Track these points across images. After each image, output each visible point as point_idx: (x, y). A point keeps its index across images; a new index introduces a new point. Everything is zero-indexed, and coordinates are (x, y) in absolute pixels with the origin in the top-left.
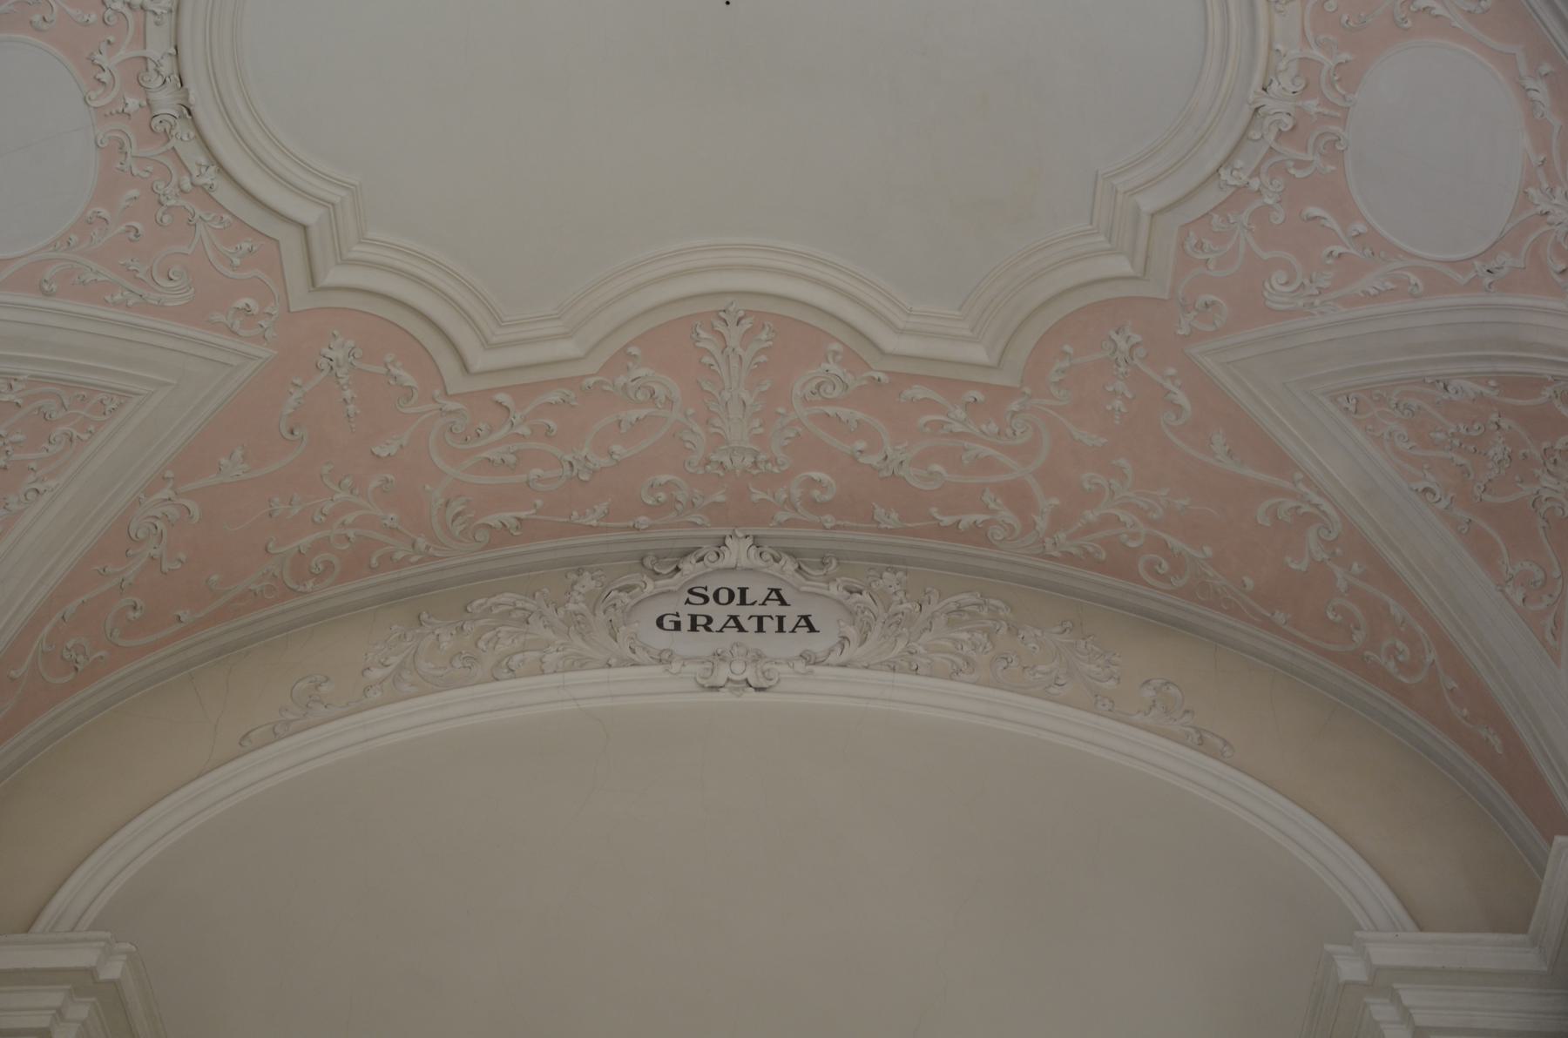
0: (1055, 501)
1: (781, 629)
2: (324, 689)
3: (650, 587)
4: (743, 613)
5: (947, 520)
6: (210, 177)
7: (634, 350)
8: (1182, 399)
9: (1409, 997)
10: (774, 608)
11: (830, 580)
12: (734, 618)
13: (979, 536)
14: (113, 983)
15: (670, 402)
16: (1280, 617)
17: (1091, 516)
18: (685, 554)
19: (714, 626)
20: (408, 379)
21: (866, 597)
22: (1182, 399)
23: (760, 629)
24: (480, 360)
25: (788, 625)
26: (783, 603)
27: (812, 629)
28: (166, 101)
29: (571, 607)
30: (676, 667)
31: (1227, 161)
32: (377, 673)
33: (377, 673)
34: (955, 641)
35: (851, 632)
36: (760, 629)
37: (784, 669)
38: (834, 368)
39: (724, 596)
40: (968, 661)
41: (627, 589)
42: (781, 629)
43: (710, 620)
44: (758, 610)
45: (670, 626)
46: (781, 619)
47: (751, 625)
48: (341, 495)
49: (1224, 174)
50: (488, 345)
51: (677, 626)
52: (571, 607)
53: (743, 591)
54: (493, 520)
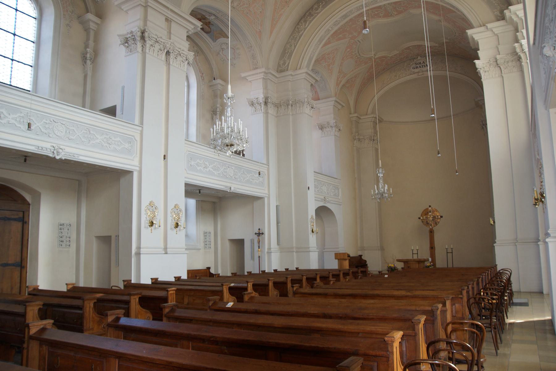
1: (424, 67)
3: (412, 63)
4: (421, 65)
6: (364, 58)
10: (423, 64)
12: (420, 66)
18: (414, 58)
19: (418, 67)
23: (423, 67)
25: (425, 66)
26: (424, 63)
29: (404, 68)
32: (388, 79)
36: (423, 67)
44: (422, 65)
46: (424, 65)
47: (421, 67)
51: (415, 68)
52: (404, 68)
53: (420, 63)
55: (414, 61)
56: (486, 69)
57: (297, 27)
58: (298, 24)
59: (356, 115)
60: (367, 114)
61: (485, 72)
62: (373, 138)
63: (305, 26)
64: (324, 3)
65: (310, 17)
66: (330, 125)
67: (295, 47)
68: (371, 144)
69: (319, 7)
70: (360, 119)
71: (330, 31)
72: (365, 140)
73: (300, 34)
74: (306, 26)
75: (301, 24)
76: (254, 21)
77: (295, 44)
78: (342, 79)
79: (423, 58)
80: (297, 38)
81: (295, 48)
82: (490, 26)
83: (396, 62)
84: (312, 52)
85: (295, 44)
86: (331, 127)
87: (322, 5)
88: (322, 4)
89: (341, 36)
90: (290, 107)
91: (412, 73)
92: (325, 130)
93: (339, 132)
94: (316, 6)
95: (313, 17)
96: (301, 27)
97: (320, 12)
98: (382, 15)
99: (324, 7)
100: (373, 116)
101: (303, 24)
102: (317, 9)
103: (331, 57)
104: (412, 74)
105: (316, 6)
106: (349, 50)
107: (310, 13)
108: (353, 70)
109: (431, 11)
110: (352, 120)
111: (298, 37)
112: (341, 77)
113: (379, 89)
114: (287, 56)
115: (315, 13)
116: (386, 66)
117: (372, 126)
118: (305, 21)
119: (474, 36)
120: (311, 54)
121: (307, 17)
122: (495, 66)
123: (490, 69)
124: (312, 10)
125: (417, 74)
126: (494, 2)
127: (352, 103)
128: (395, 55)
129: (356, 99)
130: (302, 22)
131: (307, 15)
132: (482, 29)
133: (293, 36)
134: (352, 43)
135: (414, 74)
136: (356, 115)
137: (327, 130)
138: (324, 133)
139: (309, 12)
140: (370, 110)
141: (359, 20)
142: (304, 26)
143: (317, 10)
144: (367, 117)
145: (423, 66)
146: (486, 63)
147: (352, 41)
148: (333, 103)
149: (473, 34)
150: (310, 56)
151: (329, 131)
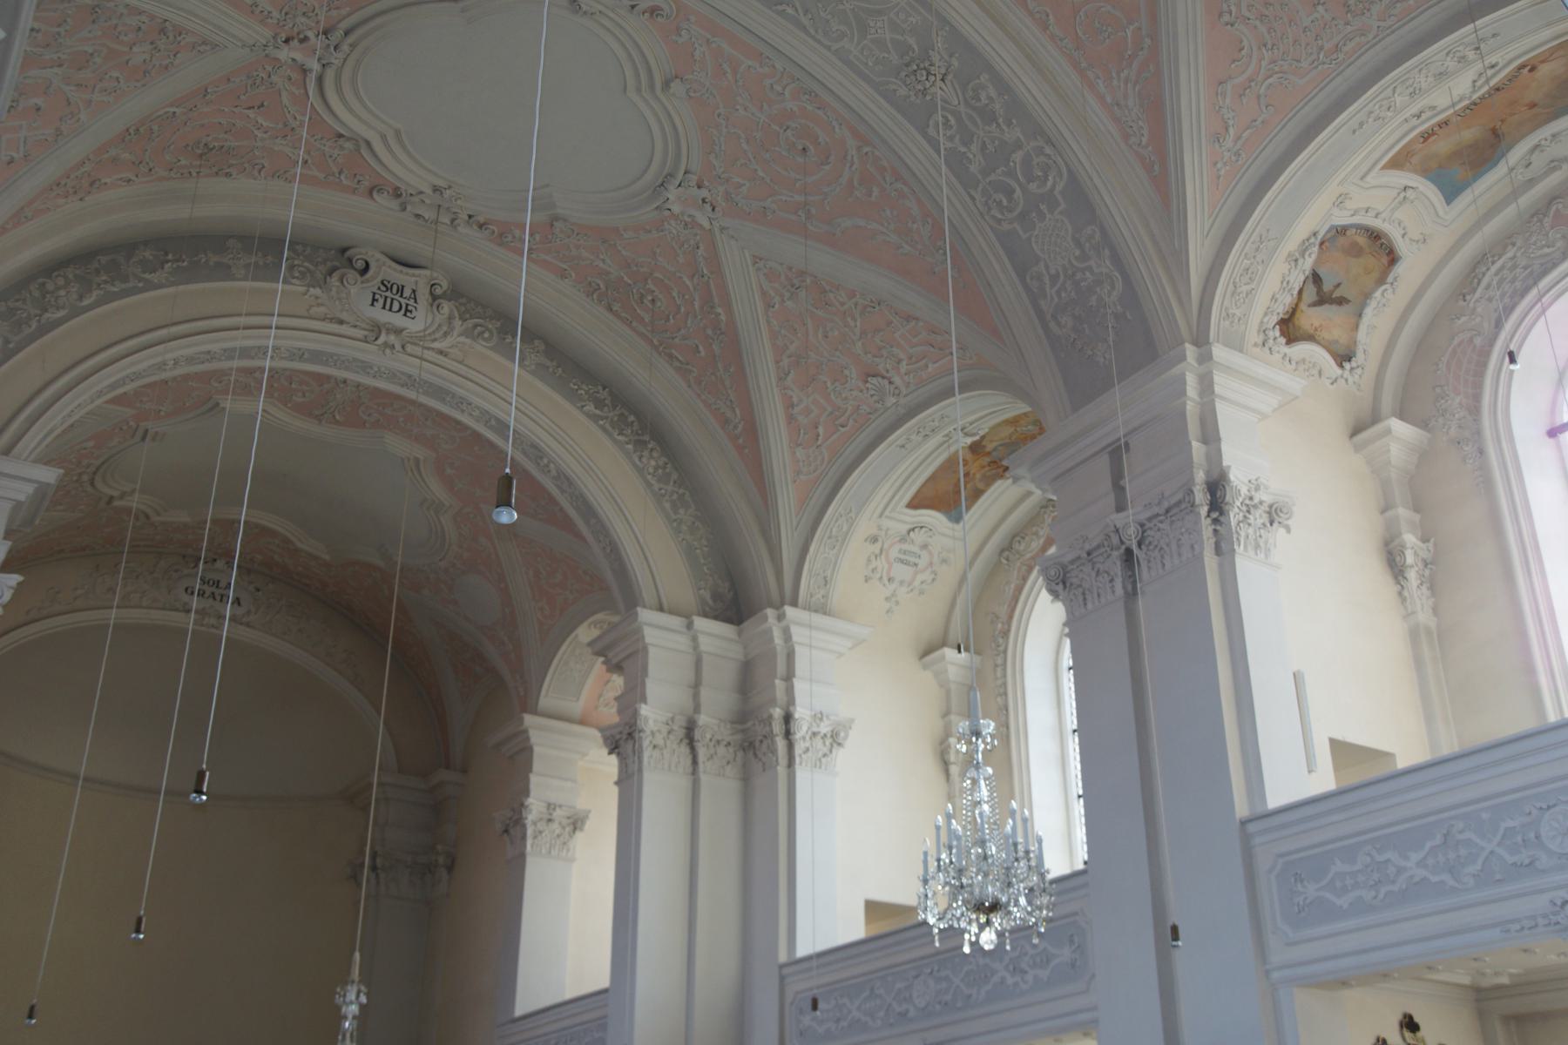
4: (217, 592)
12: (213, 593)
19: (206, 595)
21: (260, 593)
36: (221, 600)
39: (211, 583)
41: (176, 571)
43: (204, 593)
47: (218, 598)
53: (218, 582)
56: (659, 740)
57: (41, 280)
61: (655, 747)
63: (81, 298)
64: (185, 263)
69: (163, 268)
73: (47, 315)
74: (86, 302)
75: (61, 281)
80: (30, 327)
82: (701, 623)
85: (11, 346)
88: (177, 261)
94: (148, 254)
95: (123, 286)
96: (62, 293)
97: (160, 286)
104: (177, 610)
109: (449, 471)
111: (34, 325)
119: (647, 631)
121: (97, 272)
122: (681, 740)
123: (668, 742)
126: (702, 561)
130: (71, 276)
132: (676, 622)
142: (75, 296)
143: (151, 273)
146: (663, 723)
149: (646, 624)
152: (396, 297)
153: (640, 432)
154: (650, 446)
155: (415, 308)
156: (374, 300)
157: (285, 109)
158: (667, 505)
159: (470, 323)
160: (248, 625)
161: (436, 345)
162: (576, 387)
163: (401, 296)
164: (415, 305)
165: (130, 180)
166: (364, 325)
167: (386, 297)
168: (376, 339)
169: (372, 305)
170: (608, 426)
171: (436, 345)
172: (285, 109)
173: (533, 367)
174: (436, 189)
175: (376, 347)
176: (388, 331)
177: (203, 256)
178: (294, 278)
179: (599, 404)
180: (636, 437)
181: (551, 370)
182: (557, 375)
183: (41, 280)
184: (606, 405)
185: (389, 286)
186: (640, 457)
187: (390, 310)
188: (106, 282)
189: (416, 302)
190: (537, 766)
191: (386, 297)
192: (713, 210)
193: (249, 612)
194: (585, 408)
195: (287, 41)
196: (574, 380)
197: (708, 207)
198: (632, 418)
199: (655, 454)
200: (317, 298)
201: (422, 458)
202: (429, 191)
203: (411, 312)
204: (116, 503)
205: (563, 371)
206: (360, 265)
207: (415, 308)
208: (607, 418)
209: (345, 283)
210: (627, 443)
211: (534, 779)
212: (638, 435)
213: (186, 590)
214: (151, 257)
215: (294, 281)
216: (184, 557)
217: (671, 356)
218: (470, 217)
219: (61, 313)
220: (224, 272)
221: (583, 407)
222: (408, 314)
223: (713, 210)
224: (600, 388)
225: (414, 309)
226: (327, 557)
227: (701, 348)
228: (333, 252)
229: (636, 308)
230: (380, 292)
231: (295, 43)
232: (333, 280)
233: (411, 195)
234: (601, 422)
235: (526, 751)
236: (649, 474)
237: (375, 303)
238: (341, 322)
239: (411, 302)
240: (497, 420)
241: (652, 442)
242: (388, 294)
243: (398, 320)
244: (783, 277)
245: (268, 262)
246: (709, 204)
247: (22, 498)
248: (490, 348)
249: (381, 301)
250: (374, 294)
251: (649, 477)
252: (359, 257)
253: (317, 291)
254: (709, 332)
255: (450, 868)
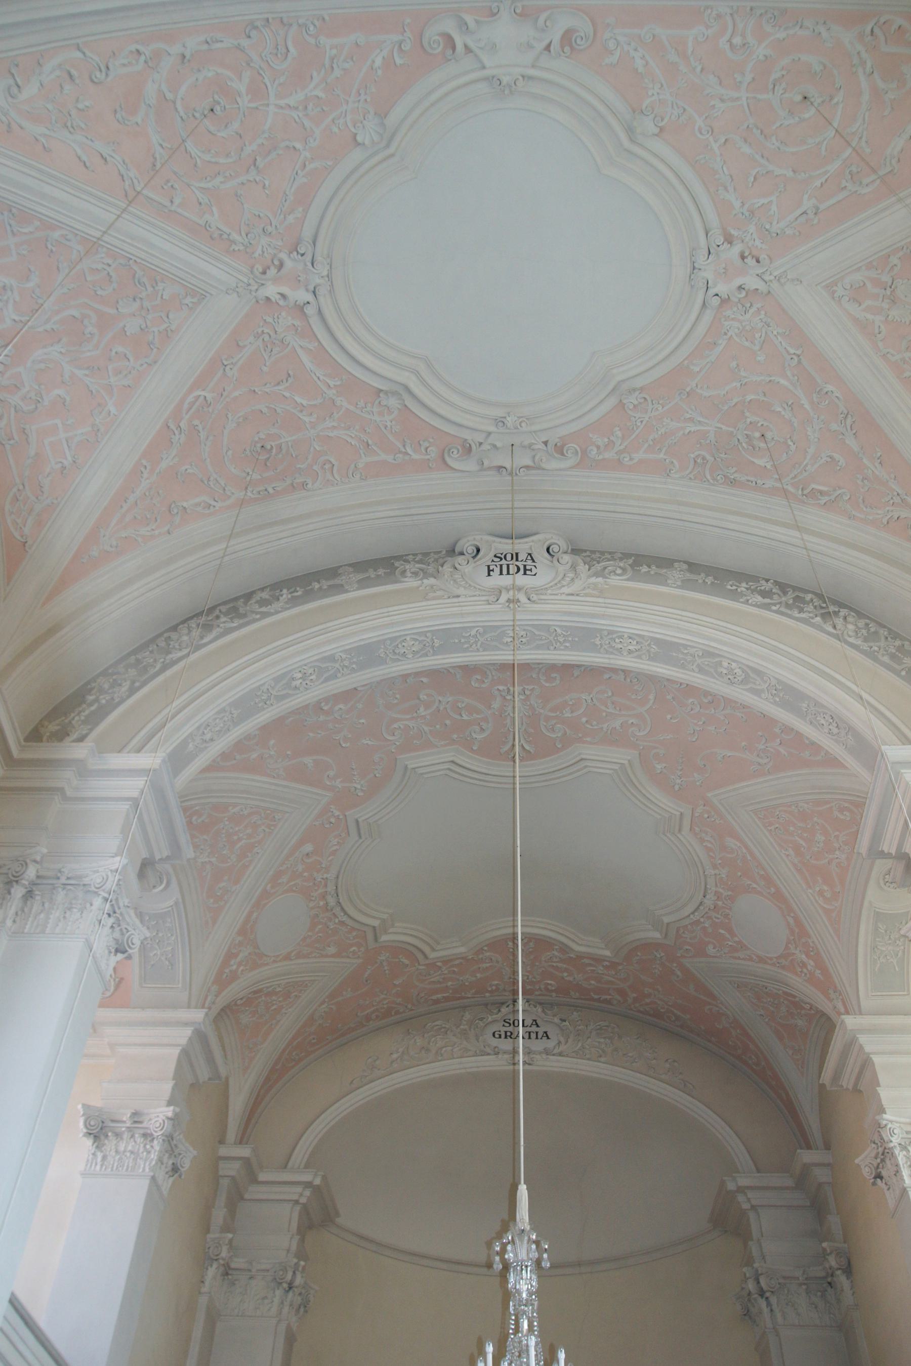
0: (635, 995)
1: (537, 1038)
2: (377, 1062)
3: (490, 1019)
5: (596, 997)
6: (345, 918)
7: (486, 948)
8: (679, 973)
9: (750, 1194)
10: (534, 1028)
11: (554, 1016)
13: (608, 1002)
14: (318, 1186)
15: (498, 962)
16: (713, 1039)
17: (648, 1001)
18: (503, 1004)
20: (406, 962)
21: (567, 1023)
22: (679, 973)
23: (530, 1038)
24: (432, 955)
25: (540, 1036)
26: (538, 1026)
27: (548, 1038)
28: (332, 901)
29: (462, 1027)
30: (500, 1056)
31: (693, 913)
32: (395, 1056)
33: (395, 1056)
34: (599, 1042)
35: (562, 1039)
36: (530, 1038)
37: (538, 1057)
38: (556, 953)
40: (603, 1051)
41: (481, 1019)
42: (537, 1038)
43: (512, 1033)
44: (529, 1029)
45: (497, 1036)
46: (537, 1033)
48: (383, 996)
49: (692, 916)
50: (433, 950)
52: (462, 1027)
54: (434, 997)
55: (499, 1011)
58: (174, 628)
59: (245, 1152)
60: (285, 1167)
62: (289, 1277)
63: (202, 638)
65: (231, 619)
66: (144, 1125)
67: (132, 691)
68: (277, 1300)
70: (254, 1181)
71: (296, 688)
72: (251, 1278)
73: (170, 656)
74: (205, 640)
76: (21, 487)
77: (137, 684)
78: (242, 968)
79: (535, 1007)
81: (129, 697)
83: (439, 996)
84: (198, 728)
85: (137, 684)
86: (145, 1135)
87: (289, 596)
89: (308, 760)
90: (18, 892)
91: (488, 1050)
92: (110, 1144)
93: (172, 1179)
94: (265, 595)
95: (241, 621)
97: (277, 612)
98: (480, 737)
99: (294, 601)
100: (307, 1177)
101: (196, 633)
102: (263, 603)
103: (240, 840)
104: (488, 1054)
105: (265, 595)
106: (308, 848)
107: (235, 609)
108: (287, 957)
109: (659, 767)
110: (221, 1173)
112: (241, 956)
113: (352, 1082)
114: (87, 712)
115: (253, 612)
116: (399, 1000)
117: (294, 1225)
118: (208, 627)
120: (191, 736)
121: (218, 617)
124: (246, 603)
125: (506, 1056)
127: (238, 1104)
128: (445, 962)
129: (256, 1099)
130: (194, 626)
131: (220, 611)
133: (139, 657)
134: (333, 820)
135: (497, 1054)
136: (245, 1152)
137: (122, 1148)
138: (104, 1158)
139: (231, 605)
140: (300, 1155)
141: (396, 726)
144: (286, 1177)
145: (533, 1036)
147: (337, 813)
148: (183, 1035)
150: (185, 743)
151: (132, 1152)
152: (511, 562)
153: (824, 605)
154: (842, 614)
155: (535, 566)
156: (489, 571)
157: (313, 375)
158: (886, 659)
159: (598, 567)
160: (560, 1054)
161: (566, 590)
162: (734, 588)
163: (517, 560)
164: (534, 564)
165: (209, 506)
166: (484, 593)
167: (501, 566)
168: (498, 600)
169: (489, 575)
170: (783, 609)
171: (566, 590)
172: (313, 375)
173: (679, 583)
174: (500, 422)
175: (501, 606)
176: (508, 590)
177: (316, 583)
178: (406, 577)
179: (765, 594)
180: (823, 611)
181: (700, 581)
182: (709, 583)
183: (166, 635)
184: (775, 594)
185: (503, 556)
186: (835, 627)
187: (508, 573)
188: (224, 622)
189: (534, 561)
190: (882, 1077)
191: (501, 566)
192: (758, 261)
193: (559, 1043)
194: (750, 601)
195: (264, 273)
196: (730, 583)
197: (750, 261)
198: (809, 597)
199: (850, 619)
200: (432, 586)
201: (626, 762)
202: (492, 428)
203: (531, 570)
204: (384, 938)
205: (715, 578)
206: (471, 550)
207: (535, 566)
208: (780, 603)
209: (457, 566)
210: (812, 618)
211: (885, 1094)
212: (822, 608)
213: (494, 1035)
214: (267, 597)
215: (406, 579)
216: (486, 1005)
217: (814, 494)
218: (546, 443)
219: (185, 652)
220: (340, 589)
221: (748, 601)
222: (528, 572)
223: (758, 261)
224: (763, 582)
225: (533, 568)
226: (607, 953)
227: (837, 456)
228: (444, 552)
229: (752, 459)
230: (493, 563)
231: (272, 272)
232: (445, 567)
233: (481, 444)
234: (774, 608)
235: (866, 1064)
236: (850, 637)
237: (491, 573)
238: (458, 596)
239: (529, 562)
240: (658, 642)
241: (841, 610)
242: (504, 562)
243: (521, 579)
244: (869, 285)
245: (380, 573)
246: (750, 258)
247: (135, 794)
248: (628, 580)
249: (497, 570)
250: (489, 567)
251: (851, 640)
252: (466, 546)
253: (432, 581)
254: (834, 426)
255: (848, 1270)
